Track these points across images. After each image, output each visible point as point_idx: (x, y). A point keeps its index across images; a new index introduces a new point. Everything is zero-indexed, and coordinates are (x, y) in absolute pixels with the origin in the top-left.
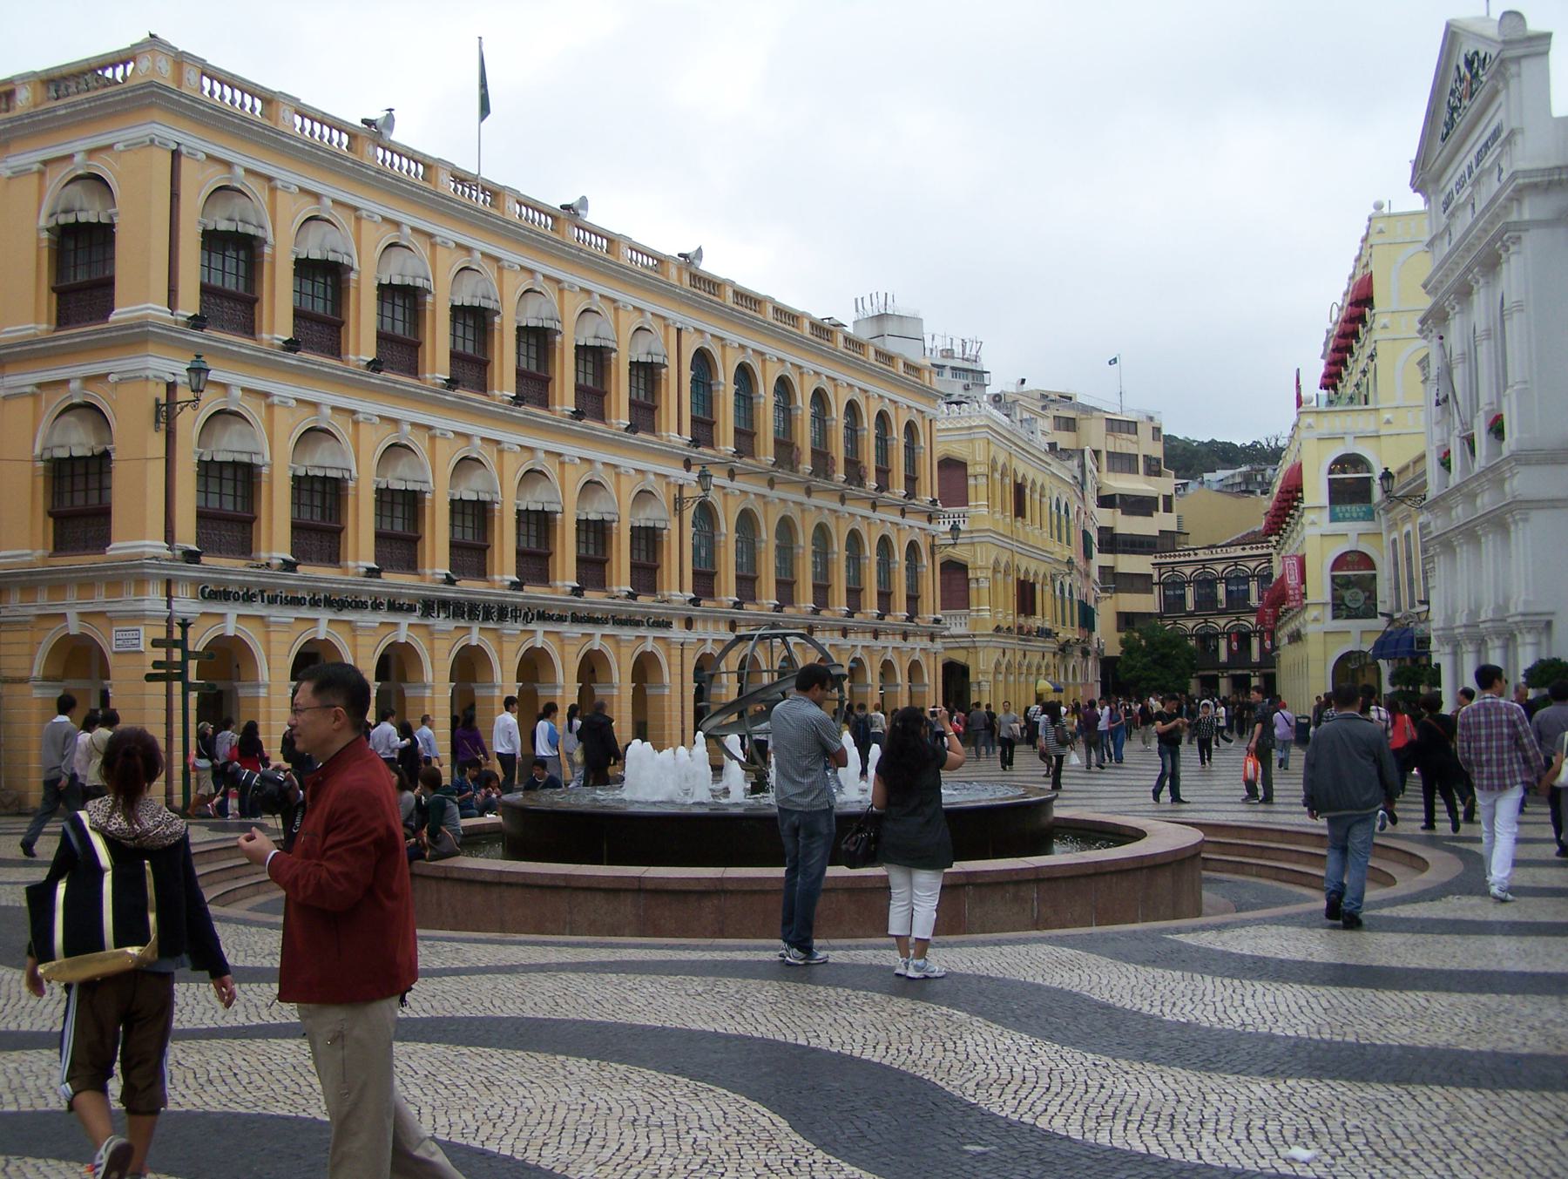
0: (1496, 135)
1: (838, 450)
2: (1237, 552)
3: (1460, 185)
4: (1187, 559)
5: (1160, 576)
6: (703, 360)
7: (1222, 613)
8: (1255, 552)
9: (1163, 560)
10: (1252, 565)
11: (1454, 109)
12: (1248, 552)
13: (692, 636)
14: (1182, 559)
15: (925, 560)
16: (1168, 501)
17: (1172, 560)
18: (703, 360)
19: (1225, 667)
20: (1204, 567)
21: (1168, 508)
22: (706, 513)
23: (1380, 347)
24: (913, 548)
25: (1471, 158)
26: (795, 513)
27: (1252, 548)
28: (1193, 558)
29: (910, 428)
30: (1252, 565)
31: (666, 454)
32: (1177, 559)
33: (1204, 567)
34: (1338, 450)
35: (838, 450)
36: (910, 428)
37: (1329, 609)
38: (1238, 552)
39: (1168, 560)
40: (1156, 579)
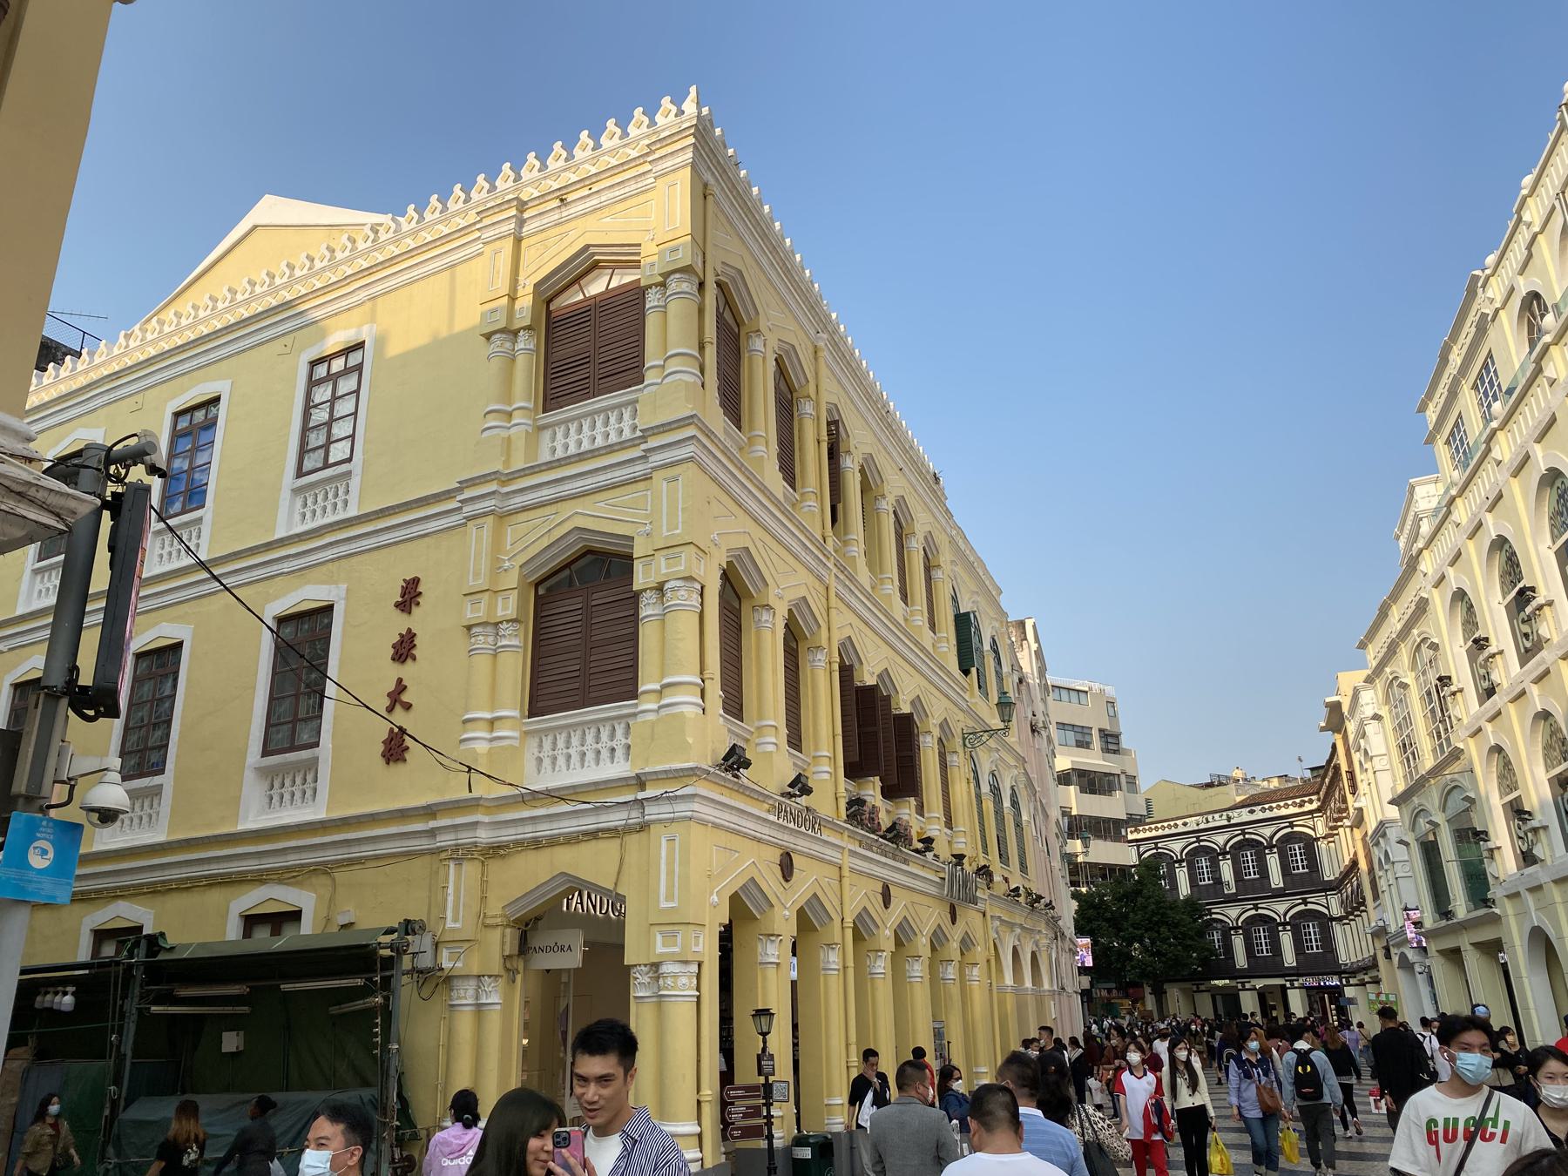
4: (1174, 831)
5: (1140, 855)
7: (1231, 900)
8: (1268, 814)
9: (1141, 835)
10: (1267, 832)
12: (1259, 815)
14: (1167, 832)
17: (1154, 834)
19: (1296, 973)
20: (1199, 841)
27: (1263, 810)
28: (1181, 829)
30: (1267, 832)
32: (1160, 833)
33: (1199, 841)
38: (1244, 816)
39: (1148, 834)
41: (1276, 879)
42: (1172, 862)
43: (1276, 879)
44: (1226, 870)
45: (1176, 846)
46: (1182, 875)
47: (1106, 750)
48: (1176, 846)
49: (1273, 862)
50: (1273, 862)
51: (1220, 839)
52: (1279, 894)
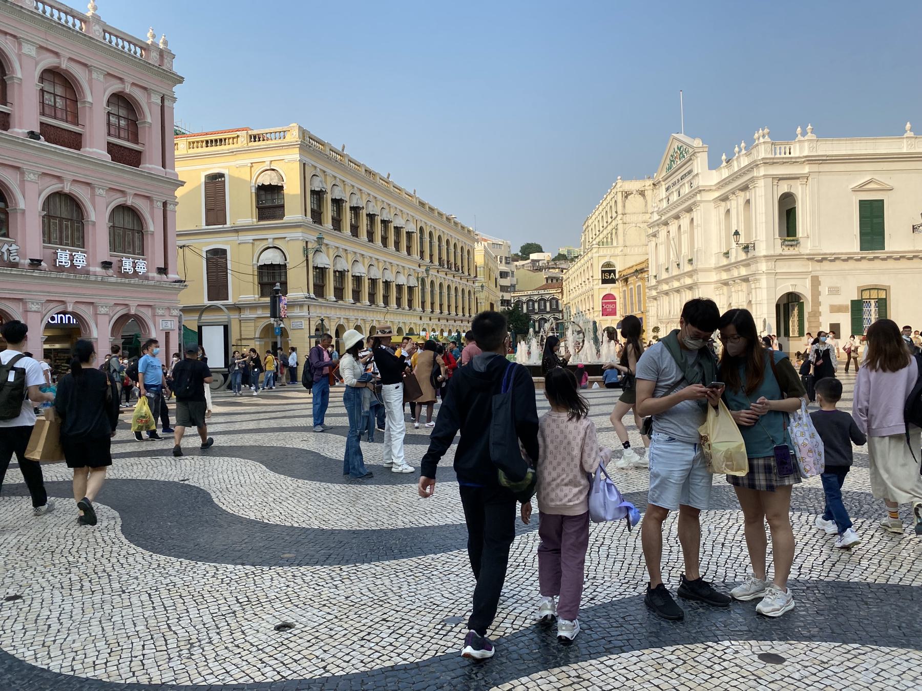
0: (690, 172)
1: (452, 260)
2: (542, 292)
3: (674, 184)
6: (421, 229)
7: (537, 313)
10: (548, 297)
11: (671, 161)
13: (422, 322)
15: (473, 297)
16: (513, 272)
18: (421, 229)
21: (513, 276)
22: (423, 280)
23: (619, 226)
24: (469, 292)
25: (679, 177)
26: (443, 281)
29: (468, 251)
30: (548, 297)
31: (413, 262)
34: (606, 260)
35: (452, 260)
36: (468, 251)
37: (601, 313)
38: (542, 292)
40: (512, 301)
41: (548, 309)
42: (523, 303)
43: (548, 309)
44: (536, 305)
45: (524, 299)
46: (525, 306)
47: (507, 263)
48: (524, 299)
49: (548, 304)
50: (548, 304)
51: (536, 298)
52: (548, 313)
